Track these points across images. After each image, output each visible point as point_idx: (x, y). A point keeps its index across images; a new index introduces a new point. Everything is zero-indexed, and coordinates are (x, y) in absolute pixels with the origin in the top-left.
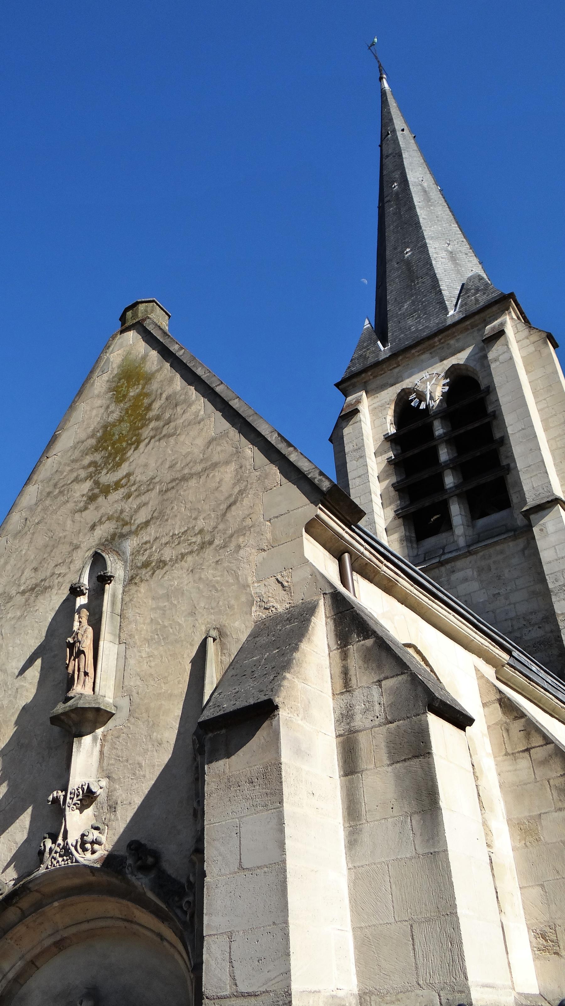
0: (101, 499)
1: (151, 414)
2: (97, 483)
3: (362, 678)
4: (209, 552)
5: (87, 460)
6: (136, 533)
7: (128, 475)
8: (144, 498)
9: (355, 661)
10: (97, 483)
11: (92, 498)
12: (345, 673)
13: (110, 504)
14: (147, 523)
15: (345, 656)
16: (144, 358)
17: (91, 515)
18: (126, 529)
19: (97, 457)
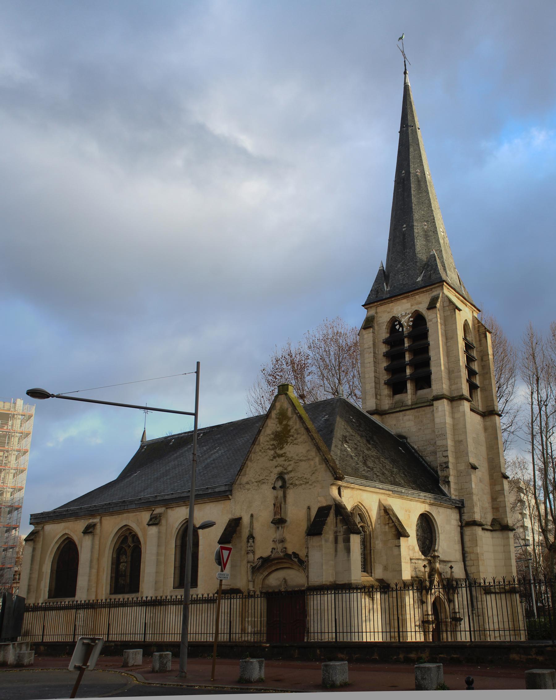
0: (277, 458)
1: (290, 434)
2: (275, 452)
3: (340, 525)
4: (307, 485)
5: (272, 443)
6: (288, 473)
7: (285, 453)
8: (290, 463)
9: (338, 521)
10: (275, 452)
11: (274, 457)
12: (336, 523)
13: (280, 460)
14: (291, 471)
15: (336, 519)
16: (287, 409)
17: (275, 463)
18: (285, 471)
19: (275, 443)
